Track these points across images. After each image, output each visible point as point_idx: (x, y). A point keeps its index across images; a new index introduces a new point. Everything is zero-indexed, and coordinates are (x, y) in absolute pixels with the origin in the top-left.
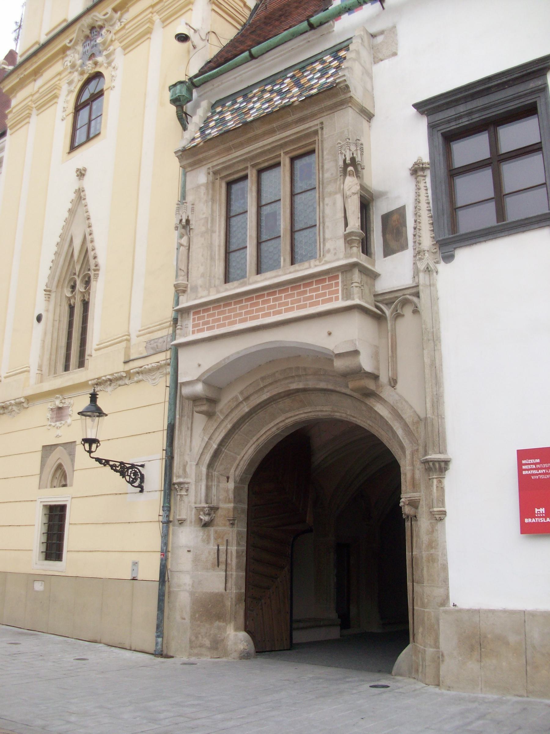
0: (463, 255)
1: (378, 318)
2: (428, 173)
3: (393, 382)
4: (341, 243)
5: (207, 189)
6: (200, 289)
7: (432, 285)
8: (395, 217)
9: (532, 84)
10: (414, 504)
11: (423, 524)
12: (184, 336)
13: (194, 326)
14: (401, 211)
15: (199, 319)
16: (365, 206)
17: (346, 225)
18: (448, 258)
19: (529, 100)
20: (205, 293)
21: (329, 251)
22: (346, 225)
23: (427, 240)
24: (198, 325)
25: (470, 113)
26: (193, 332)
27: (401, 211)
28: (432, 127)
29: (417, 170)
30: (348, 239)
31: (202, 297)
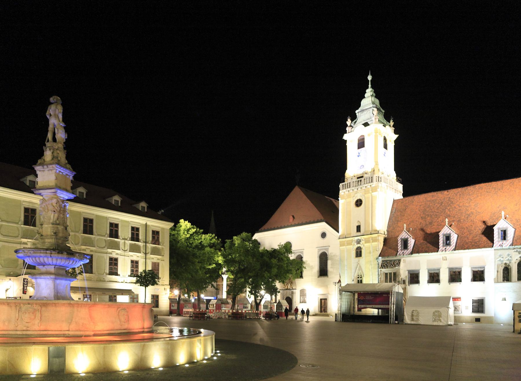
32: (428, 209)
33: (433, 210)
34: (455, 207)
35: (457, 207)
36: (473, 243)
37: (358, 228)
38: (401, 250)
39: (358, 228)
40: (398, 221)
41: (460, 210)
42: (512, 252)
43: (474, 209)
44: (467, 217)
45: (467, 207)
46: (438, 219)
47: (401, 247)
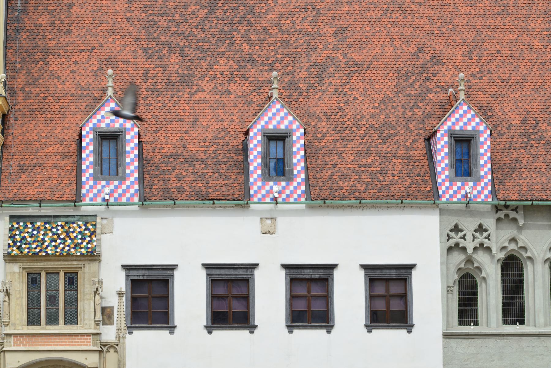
0: (136, 333)
1: (101, 352)
2: (125, 295)
4: (93, 323)
5: (19, 275)
6: (17, 326)
7: (124, 343)
8: (108, 310)
9: (169, 272)
12: (10, 346)
13: (14, 343)
14: (112, 308)
15: (17, 340)
17: (95, 315)
18: (130, 333)
19: (166, 278)
20: (20, 328)
21: (86, 324)
22: (95, 315)
23: (123, 325)
24: (17, 343)
25: (143, 275)
26: (14, 346)
27: (112, 308)
28: (127, 276)
29: (120, 294)
31: (18, 330)
32: (163, 22)
33: (184, 27)
34: (265, 30)
35: (273, 31)
36: (366, 178)
38: (96, 178)
40: (46, 51)
41: (286, 44)
42: (490, 223)
43: (336, 48)
44: (319, 76)
45: (308, 34)
46: (211, 66)
47: (95, 163)
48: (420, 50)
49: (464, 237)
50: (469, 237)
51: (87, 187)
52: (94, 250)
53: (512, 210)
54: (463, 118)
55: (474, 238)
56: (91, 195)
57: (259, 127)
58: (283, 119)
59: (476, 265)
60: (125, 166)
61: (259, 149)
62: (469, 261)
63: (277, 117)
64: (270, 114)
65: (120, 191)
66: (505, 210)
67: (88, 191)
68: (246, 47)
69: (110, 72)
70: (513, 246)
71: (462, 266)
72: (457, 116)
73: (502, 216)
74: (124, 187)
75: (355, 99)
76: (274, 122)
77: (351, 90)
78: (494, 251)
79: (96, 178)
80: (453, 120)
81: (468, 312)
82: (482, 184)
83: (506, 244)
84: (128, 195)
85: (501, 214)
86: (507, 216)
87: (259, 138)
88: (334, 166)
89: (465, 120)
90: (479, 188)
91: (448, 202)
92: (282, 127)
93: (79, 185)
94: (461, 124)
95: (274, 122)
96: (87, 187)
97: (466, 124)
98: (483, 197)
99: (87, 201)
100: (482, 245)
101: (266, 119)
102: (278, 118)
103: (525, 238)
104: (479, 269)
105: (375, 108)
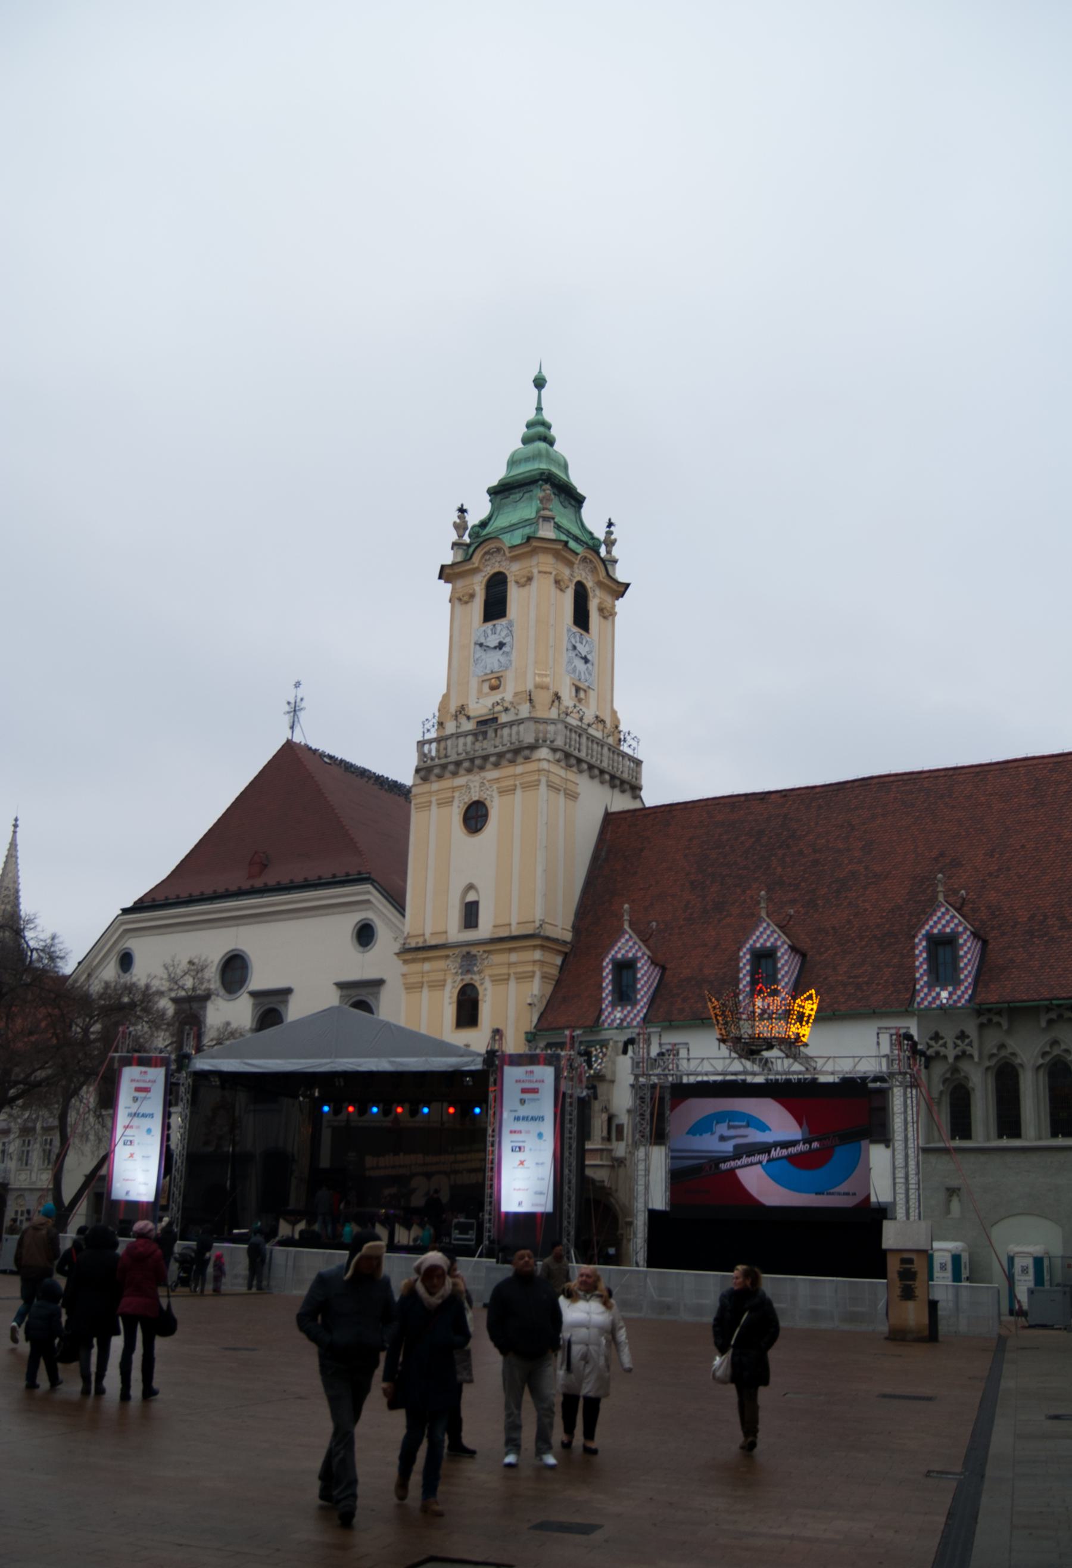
1: (612, 1167)
3: (617, 1190)
4: (599, 1139)
10: (622, 1235)
11: (625, 1241)
16: (610, 1119)
29: (629, 1111)
30: (603, 1139)
37: (471, 914)
38: (613, 1005)
39: (471, 914)
47: (613, 992)
48: (942, 855)
49: (945, 1045)
50: (950, 1045)
51: (606, 1013)
52: (600, 1070)
53: (996, 1014)
54: (944, 920)
55: (956, 1046)
56: (609, 1021)
57: (748, 946)
58: (769, 937)
59: (962, 1074)
60: (636, 991)
61: (748, 968)
62: (955, 1070)
63: (766, 935)
64: (758, 933)
65: (632, 1015)
66: (986, 1013)
67: (607, 1017)
68: (779, 869)
69: (626, 906)
70: (1056, 1051)
71: (948, 1075)
72: (935, 918)
73: (985, 1021)
74: (635, 1012)
75: (866, 910)
76: (761, 941)
77: (864, 901)
78: (976, 1059)
79: (613, 1005)
80: (931, 923)
81: (961, 1126)
82: (963, 988)
83: (995, 1051)
84: (638, 1019)
85: (984, 1019)
86: (990, 1020)
87: (748, 957)
88: (826, 979)
89: (943, 922)
90: (959, 993)
91: (928, 1009)
92: (768, 944)
93: (601, 1012)
94: (940, 926)
95: (761, 941)
96: (606, 1013)
97: (944, 926)
98: (963, 1001)
99: (606, 1025)
100: (964, 1052)
101: (754, 938)
102: (765, 936)
103: (1013, 1044)
104: (966, 1078)
105: (882, 917)
